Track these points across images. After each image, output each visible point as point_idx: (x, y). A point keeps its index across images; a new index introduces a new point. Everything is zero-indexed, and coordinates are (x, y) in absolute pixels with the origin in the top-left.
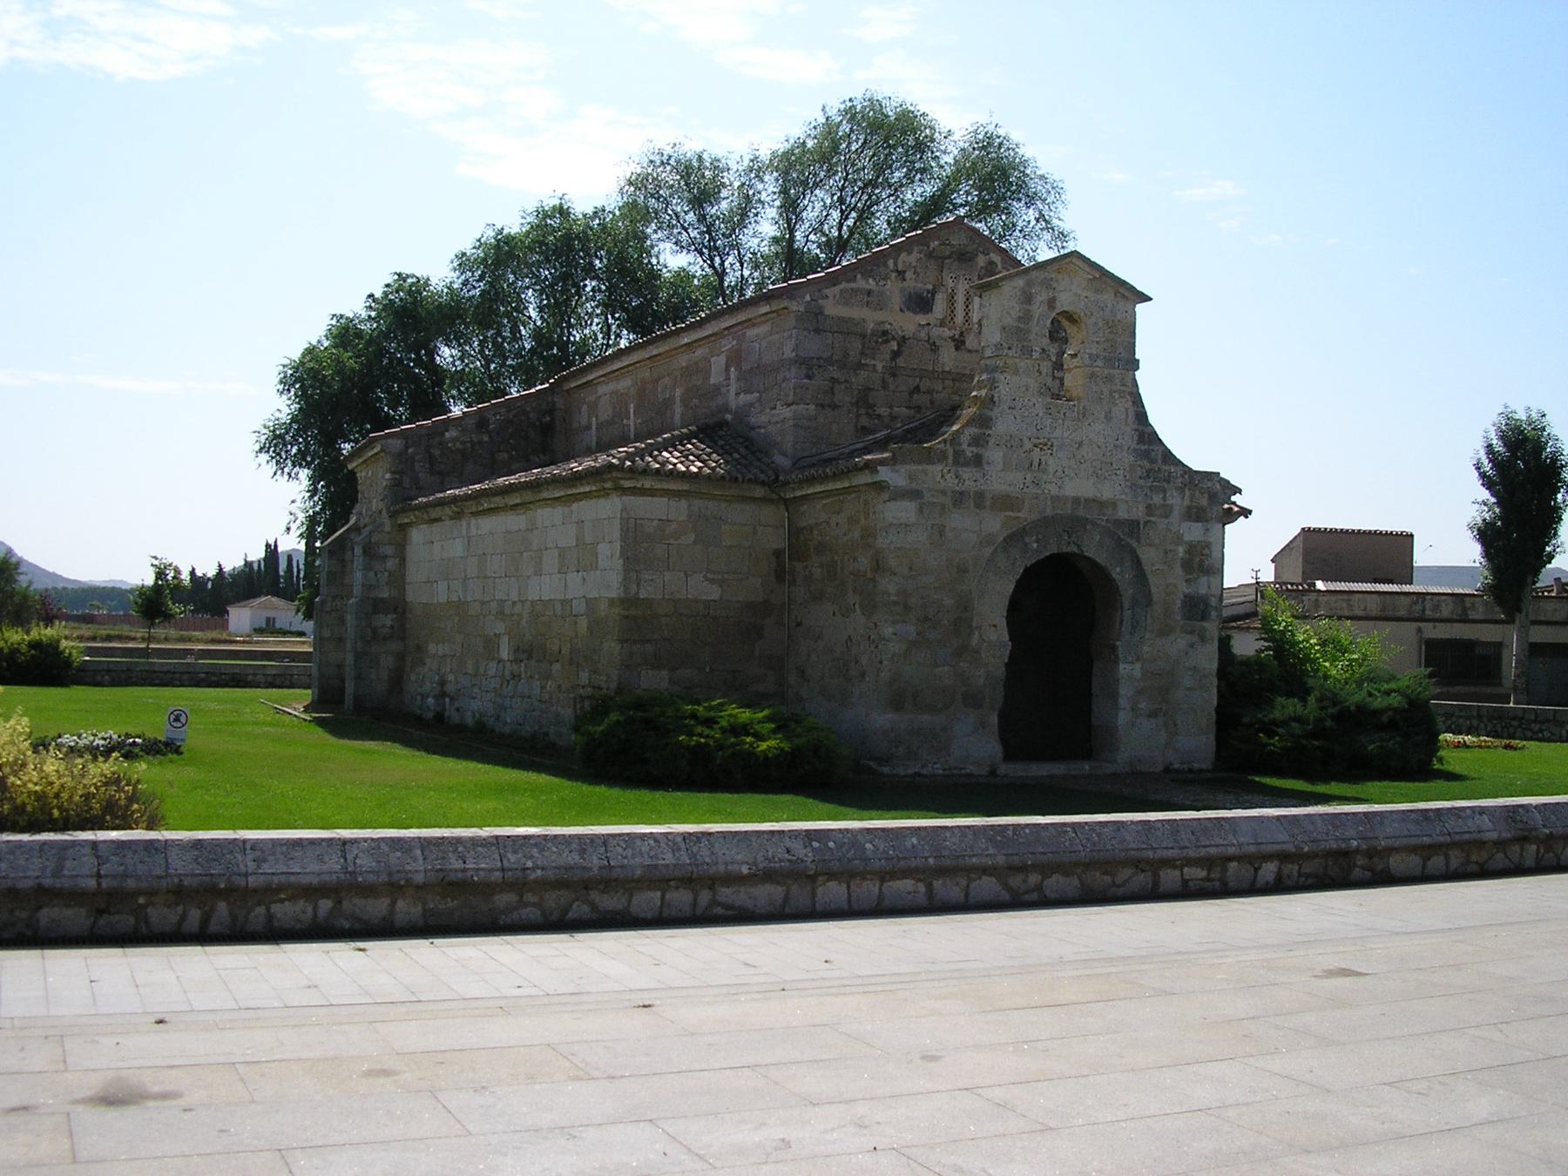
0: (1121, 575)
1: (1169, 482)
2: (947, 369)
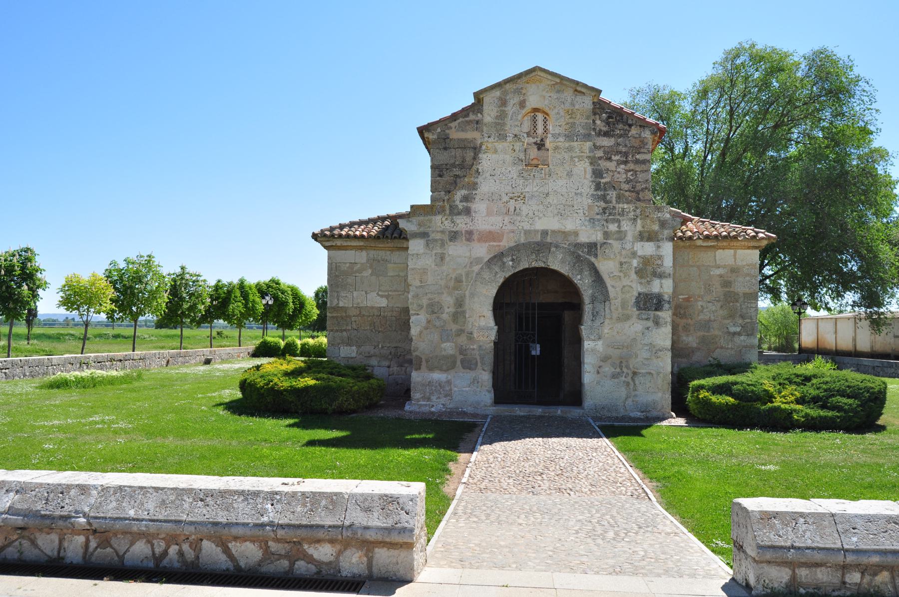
0: (583, 282)
1: (623, 215)
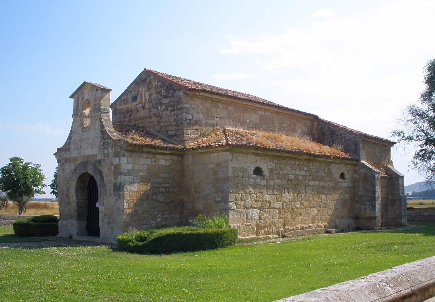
0: (97, 178)
2: (141, 116)
